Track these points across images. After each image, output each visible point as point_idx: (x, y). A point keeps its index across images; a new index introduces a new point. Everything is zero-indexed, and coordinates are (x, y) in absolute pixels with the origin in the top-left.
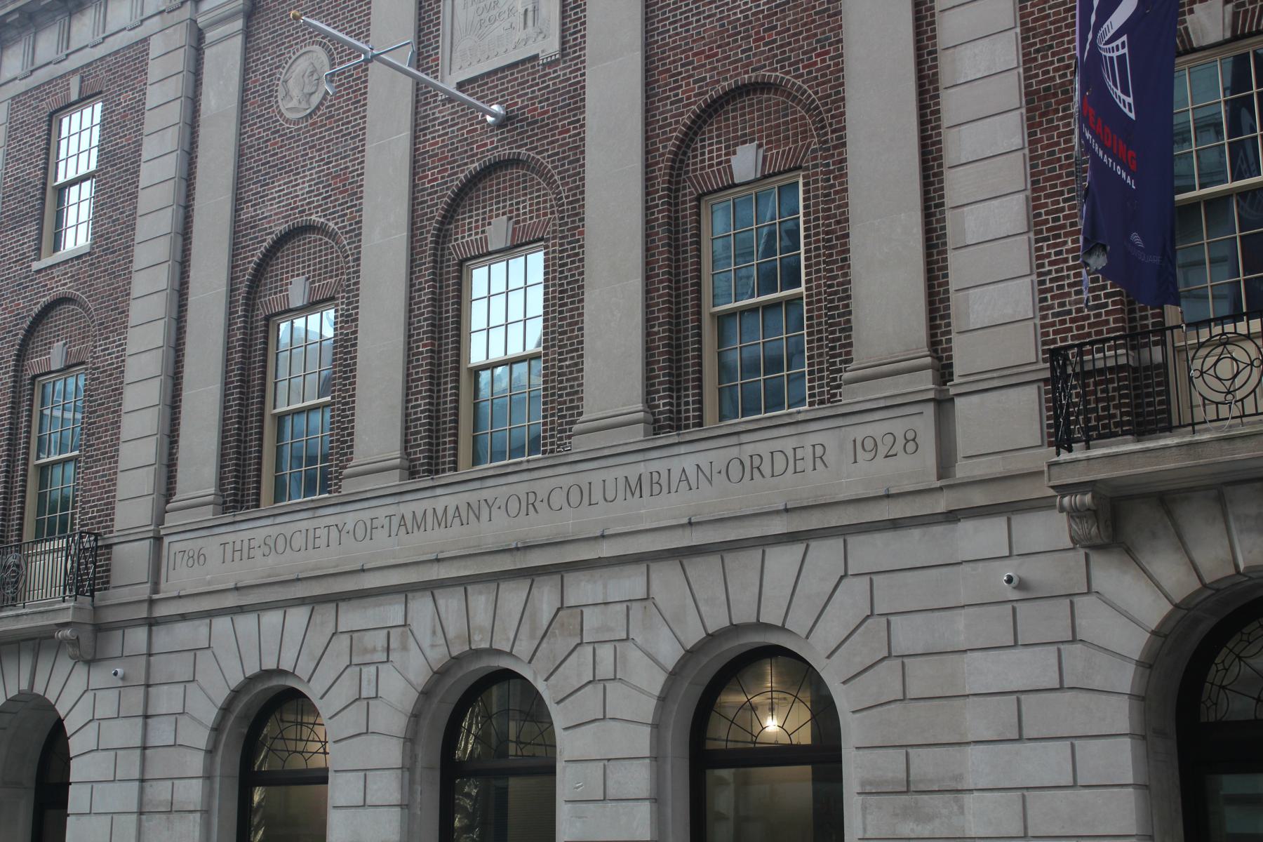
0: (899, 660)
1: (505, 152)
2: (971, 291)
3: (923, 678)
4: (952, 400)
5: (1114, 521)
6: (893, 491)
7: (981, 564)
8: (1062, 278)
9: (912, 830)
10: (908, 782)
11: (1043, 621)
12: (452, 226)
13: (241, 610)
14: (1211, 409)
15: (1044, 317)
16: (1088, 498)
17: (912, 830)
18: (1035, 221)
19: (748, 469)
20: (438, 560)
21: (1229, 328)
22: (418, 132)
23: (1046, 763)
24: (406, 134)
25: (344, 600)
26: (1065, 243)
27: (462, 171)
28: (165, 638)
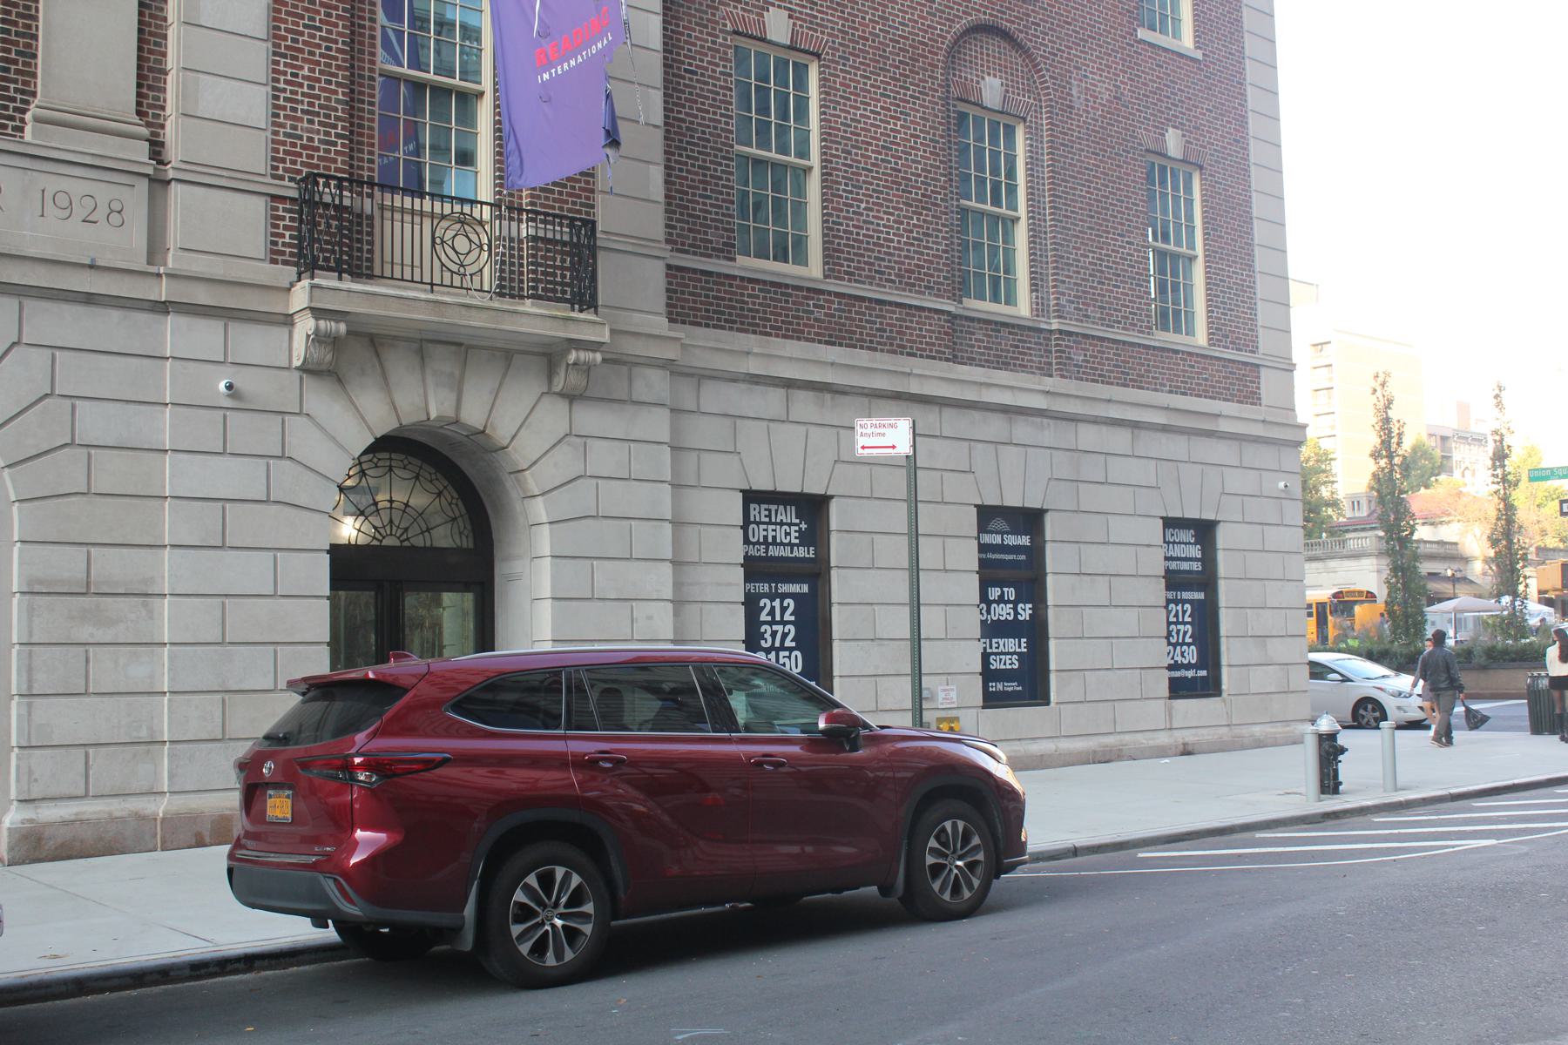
0: (85, 450)
2: (202, 76)
3: (112, 472)
4: (169, 182)
5: (349, 352)
6: (100, 263)
7: (191, 364)
8: (296, 101)
9: (92, 635)
10: (88, 583)
11: (250, 432)
14: (447, 275)
15: (276, 133)
16: (343, 327)
17: (92, 635)
18: (275, 36)
21: (467, 209)
23: (249, 572)
26: (302, 68)
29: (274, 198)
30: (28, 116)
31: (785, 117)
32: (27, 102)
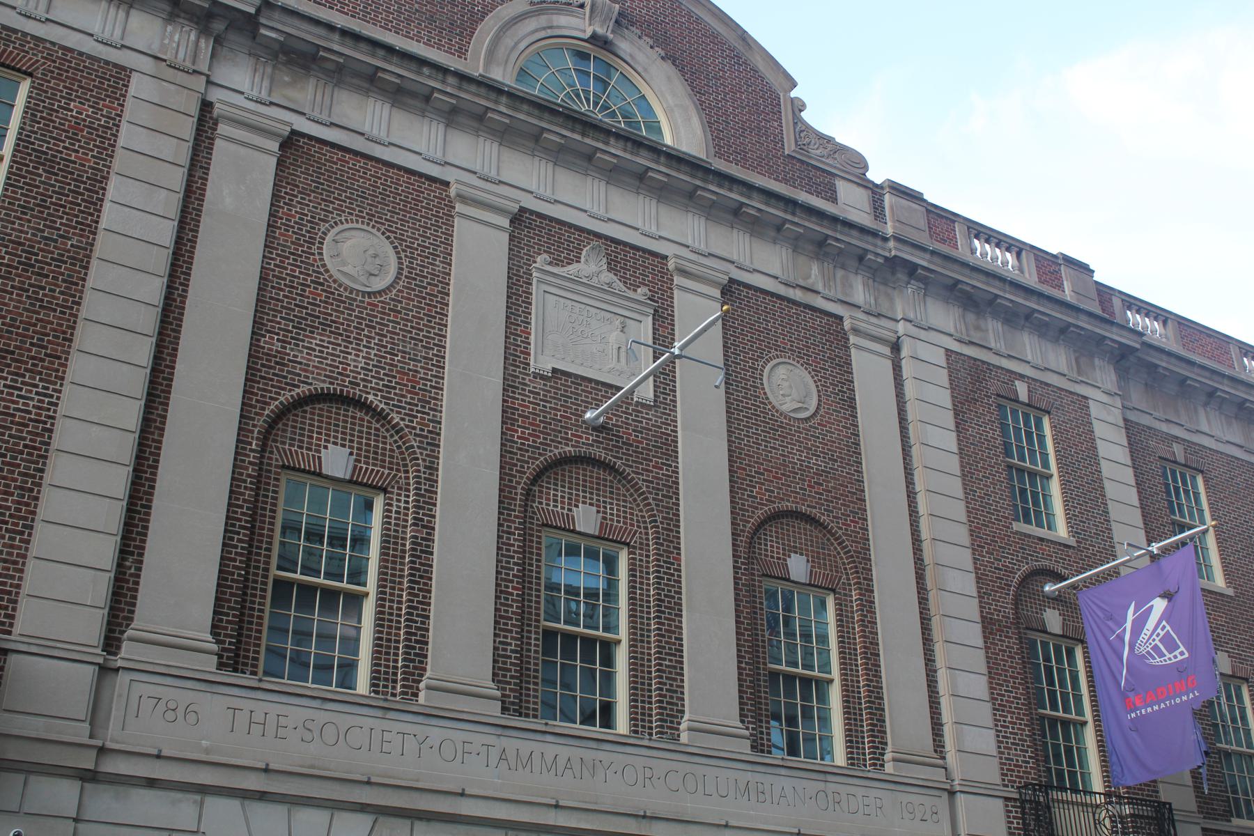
1: (599, 452)
12: (537, 489)
13: (262, 796)
19: (831, 802)
20: (557, 806)
22: (510, 386)
24: (499, 381)
25: (420, 819)
27: (556, 447)
28: (103, 802)
29: (1007, 799)
30: (422, 685)
31: (1052, 684)
32: (422, 675)
